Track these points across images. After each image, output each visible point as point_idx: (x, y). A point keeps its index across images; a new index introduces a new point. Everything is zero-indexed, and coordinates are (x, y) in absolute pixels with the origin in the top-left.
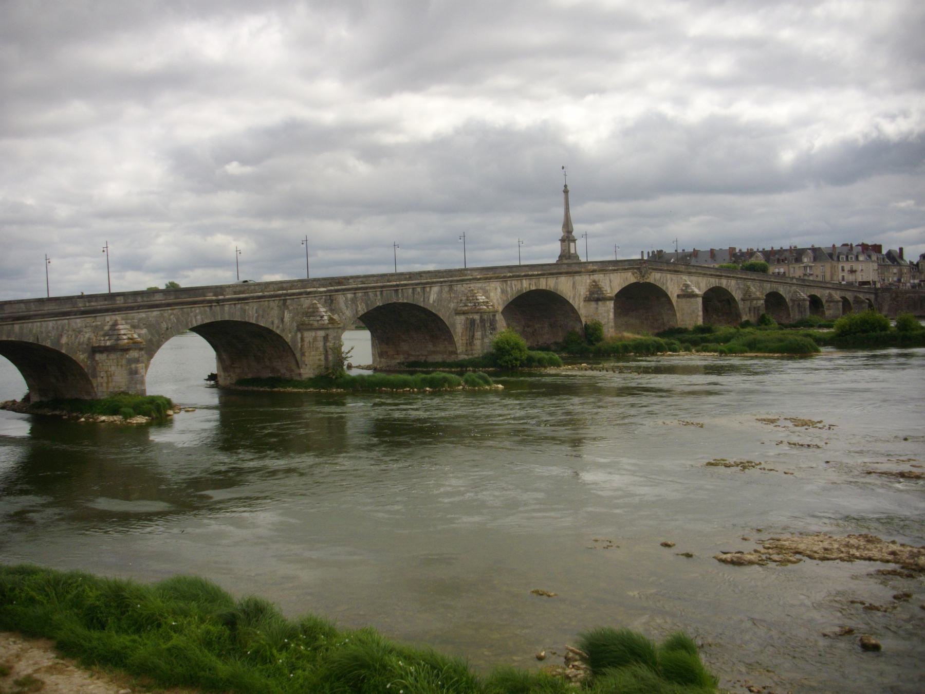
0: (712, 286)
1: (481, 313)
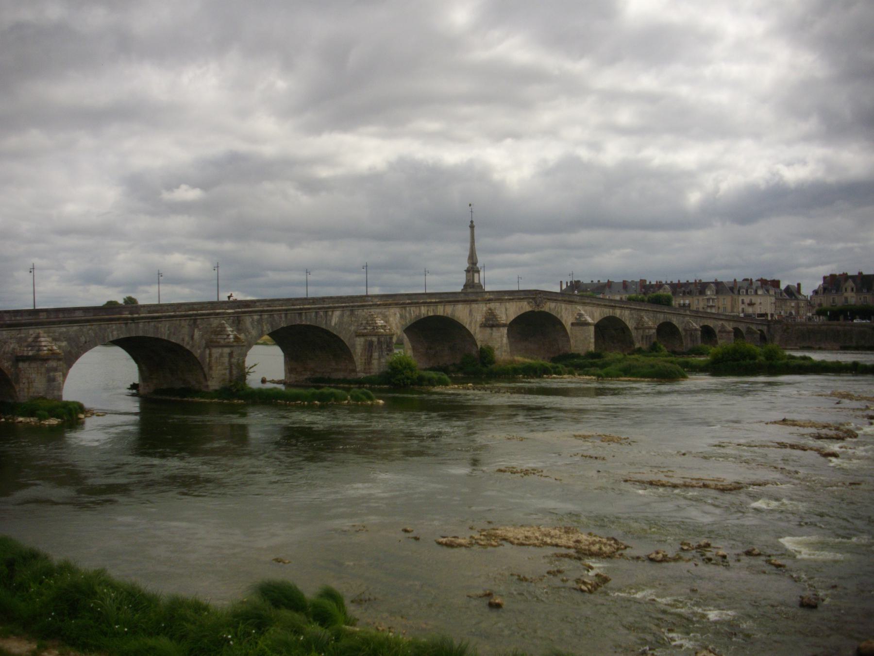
0: (605, 316)
1: (379, 336)
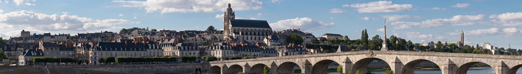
0: (416, 59)
